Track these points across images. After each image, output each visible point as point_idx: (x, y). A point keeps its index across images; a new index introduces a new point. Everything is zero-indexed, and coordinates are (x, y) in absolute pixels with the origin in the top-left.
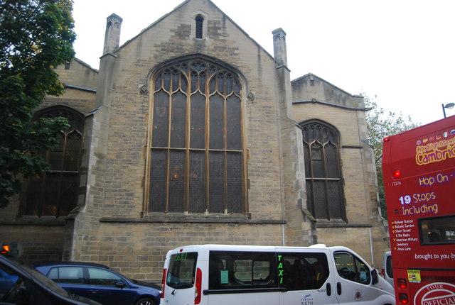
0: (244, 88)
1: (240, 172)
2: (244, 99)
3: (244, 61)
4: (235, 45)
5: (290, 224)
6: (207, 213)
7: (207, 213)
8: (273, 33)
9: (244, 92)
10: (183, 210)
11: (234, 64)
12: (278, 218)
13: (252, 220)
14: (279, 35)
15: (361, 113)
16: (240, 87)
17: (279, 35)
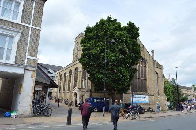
0: (147, 65)
1: (146, 84)
2: (147, 67)
3: (147, 58)
4: (145, 54)
5: (155, 96)
6: (141, 93)
7: (141, 93)
8: (152, 51)
9: (147, 66)
10: (137, 91)
11: (146, 59)
12: (153, 94)
13: (149, 94)
14: (153, 52)
15: (162, 70)
16: (146, 64)
17: (153, 52)
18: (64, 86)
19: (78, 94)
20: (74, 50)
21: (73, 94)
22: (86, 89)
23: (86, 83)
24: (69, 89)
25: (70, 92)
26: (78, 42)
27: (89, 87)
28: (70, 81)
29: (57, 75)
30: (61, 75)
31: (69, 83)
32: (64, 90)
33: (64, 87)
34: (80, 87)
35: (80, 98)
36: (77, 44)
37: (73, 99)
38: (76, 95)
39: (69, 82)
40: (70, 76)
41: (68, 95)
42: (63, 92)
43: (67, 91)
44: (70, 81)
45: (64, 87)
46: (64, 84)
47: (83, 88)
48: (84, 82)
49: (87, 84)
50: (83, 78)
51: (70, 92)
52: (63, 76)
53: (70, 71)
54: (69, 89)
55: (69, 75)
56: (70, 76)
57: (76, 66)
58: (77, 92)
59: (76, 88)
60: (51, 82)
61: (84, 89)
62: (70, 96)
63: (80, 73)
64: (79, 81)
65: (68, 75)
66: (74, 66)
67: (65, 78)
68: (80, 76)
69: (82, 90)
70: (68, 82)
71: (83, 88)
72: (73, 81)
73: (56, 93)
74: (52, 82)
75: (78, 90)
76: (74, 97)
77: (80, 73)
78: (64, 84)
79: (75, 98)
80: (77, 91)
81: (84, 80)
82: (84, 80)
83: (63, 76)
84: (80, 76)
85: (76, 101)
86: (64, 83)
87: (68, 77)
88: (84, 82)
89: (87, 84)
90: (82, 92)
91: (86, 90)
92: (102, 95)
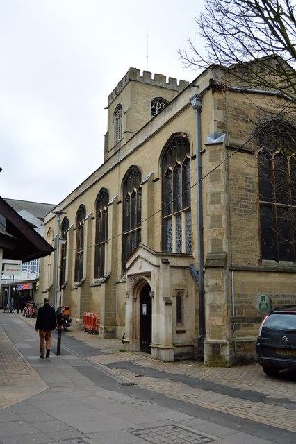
18: (77, 262)
19: (160, 284)
20: (107, 136)
21: (125, 288)
22: (195, 252)
23: (189, 229)
24: (99, 271)
25: (106, 282)
26: (119, 107)
27: (216, 243)
28: (101, 236)
29: (48, 226)
30: (66, 221)
31: (97, 248)
32: (79, 276)
33: (79, 267)
34: (158, 248)
35: (168, 303)
36: (115, 113)
37: (130, 309)
38: (143, 292)
39: (97, 240)
40: (102, 219)
41: (99, 295)
42: (74, 284)
43: (93, 281)
44: (101, 236)
45: (79, 267)
46: (79, 255)
47: (174, 251)
48: (179, 228)
49: (201, 229)
50: (165, 210)
51: (106, 282)
52: (73, 222)
53: (103, 196)
54: (99, 271)
55: (98, 215)
56: (102, 219)
57: (125, 167)
58: (148, 274)
59: (140, 252)
60: (10, 227)
61: (179, 255)
62: (110, 299)
63: (151, 190)
64: (151, 216)
65: (94, 215)
66: (117, 168)
67: (80, 227)
68: (151, 199)
69: (173, 261)
70: (94, 243)
71: (174, 251)
72: (115, 230)
73: (49, 290)
74: (14, 221)
75: (155, 260)
76: (134, 300)
77: (151, 190)
78: (79, 255)
79: (138, 305)
80: (146, 268)
81: (176, 216)
82: (179, 216)
83: (73, 222)
84: (151, 199)
85: (146, 322)
86: (78, 249)
87: (94, 221)
88: (179, 228)
89: (201, 229)
90: (174, 271)
91: (197, 261)
92: (282, 285)
